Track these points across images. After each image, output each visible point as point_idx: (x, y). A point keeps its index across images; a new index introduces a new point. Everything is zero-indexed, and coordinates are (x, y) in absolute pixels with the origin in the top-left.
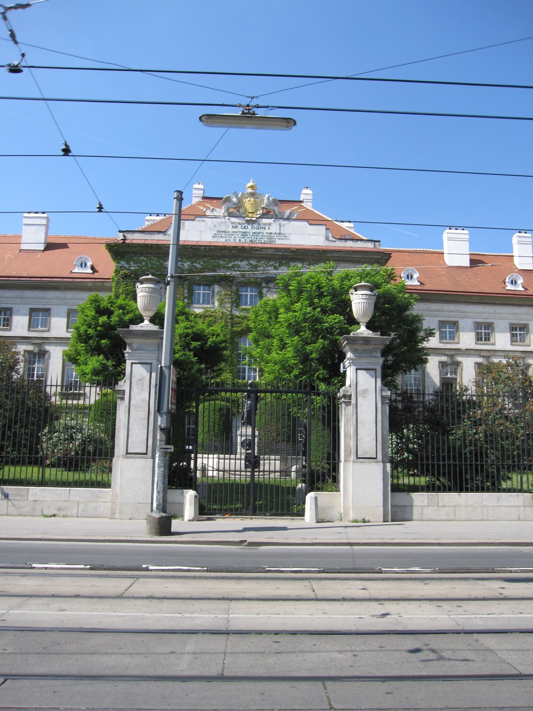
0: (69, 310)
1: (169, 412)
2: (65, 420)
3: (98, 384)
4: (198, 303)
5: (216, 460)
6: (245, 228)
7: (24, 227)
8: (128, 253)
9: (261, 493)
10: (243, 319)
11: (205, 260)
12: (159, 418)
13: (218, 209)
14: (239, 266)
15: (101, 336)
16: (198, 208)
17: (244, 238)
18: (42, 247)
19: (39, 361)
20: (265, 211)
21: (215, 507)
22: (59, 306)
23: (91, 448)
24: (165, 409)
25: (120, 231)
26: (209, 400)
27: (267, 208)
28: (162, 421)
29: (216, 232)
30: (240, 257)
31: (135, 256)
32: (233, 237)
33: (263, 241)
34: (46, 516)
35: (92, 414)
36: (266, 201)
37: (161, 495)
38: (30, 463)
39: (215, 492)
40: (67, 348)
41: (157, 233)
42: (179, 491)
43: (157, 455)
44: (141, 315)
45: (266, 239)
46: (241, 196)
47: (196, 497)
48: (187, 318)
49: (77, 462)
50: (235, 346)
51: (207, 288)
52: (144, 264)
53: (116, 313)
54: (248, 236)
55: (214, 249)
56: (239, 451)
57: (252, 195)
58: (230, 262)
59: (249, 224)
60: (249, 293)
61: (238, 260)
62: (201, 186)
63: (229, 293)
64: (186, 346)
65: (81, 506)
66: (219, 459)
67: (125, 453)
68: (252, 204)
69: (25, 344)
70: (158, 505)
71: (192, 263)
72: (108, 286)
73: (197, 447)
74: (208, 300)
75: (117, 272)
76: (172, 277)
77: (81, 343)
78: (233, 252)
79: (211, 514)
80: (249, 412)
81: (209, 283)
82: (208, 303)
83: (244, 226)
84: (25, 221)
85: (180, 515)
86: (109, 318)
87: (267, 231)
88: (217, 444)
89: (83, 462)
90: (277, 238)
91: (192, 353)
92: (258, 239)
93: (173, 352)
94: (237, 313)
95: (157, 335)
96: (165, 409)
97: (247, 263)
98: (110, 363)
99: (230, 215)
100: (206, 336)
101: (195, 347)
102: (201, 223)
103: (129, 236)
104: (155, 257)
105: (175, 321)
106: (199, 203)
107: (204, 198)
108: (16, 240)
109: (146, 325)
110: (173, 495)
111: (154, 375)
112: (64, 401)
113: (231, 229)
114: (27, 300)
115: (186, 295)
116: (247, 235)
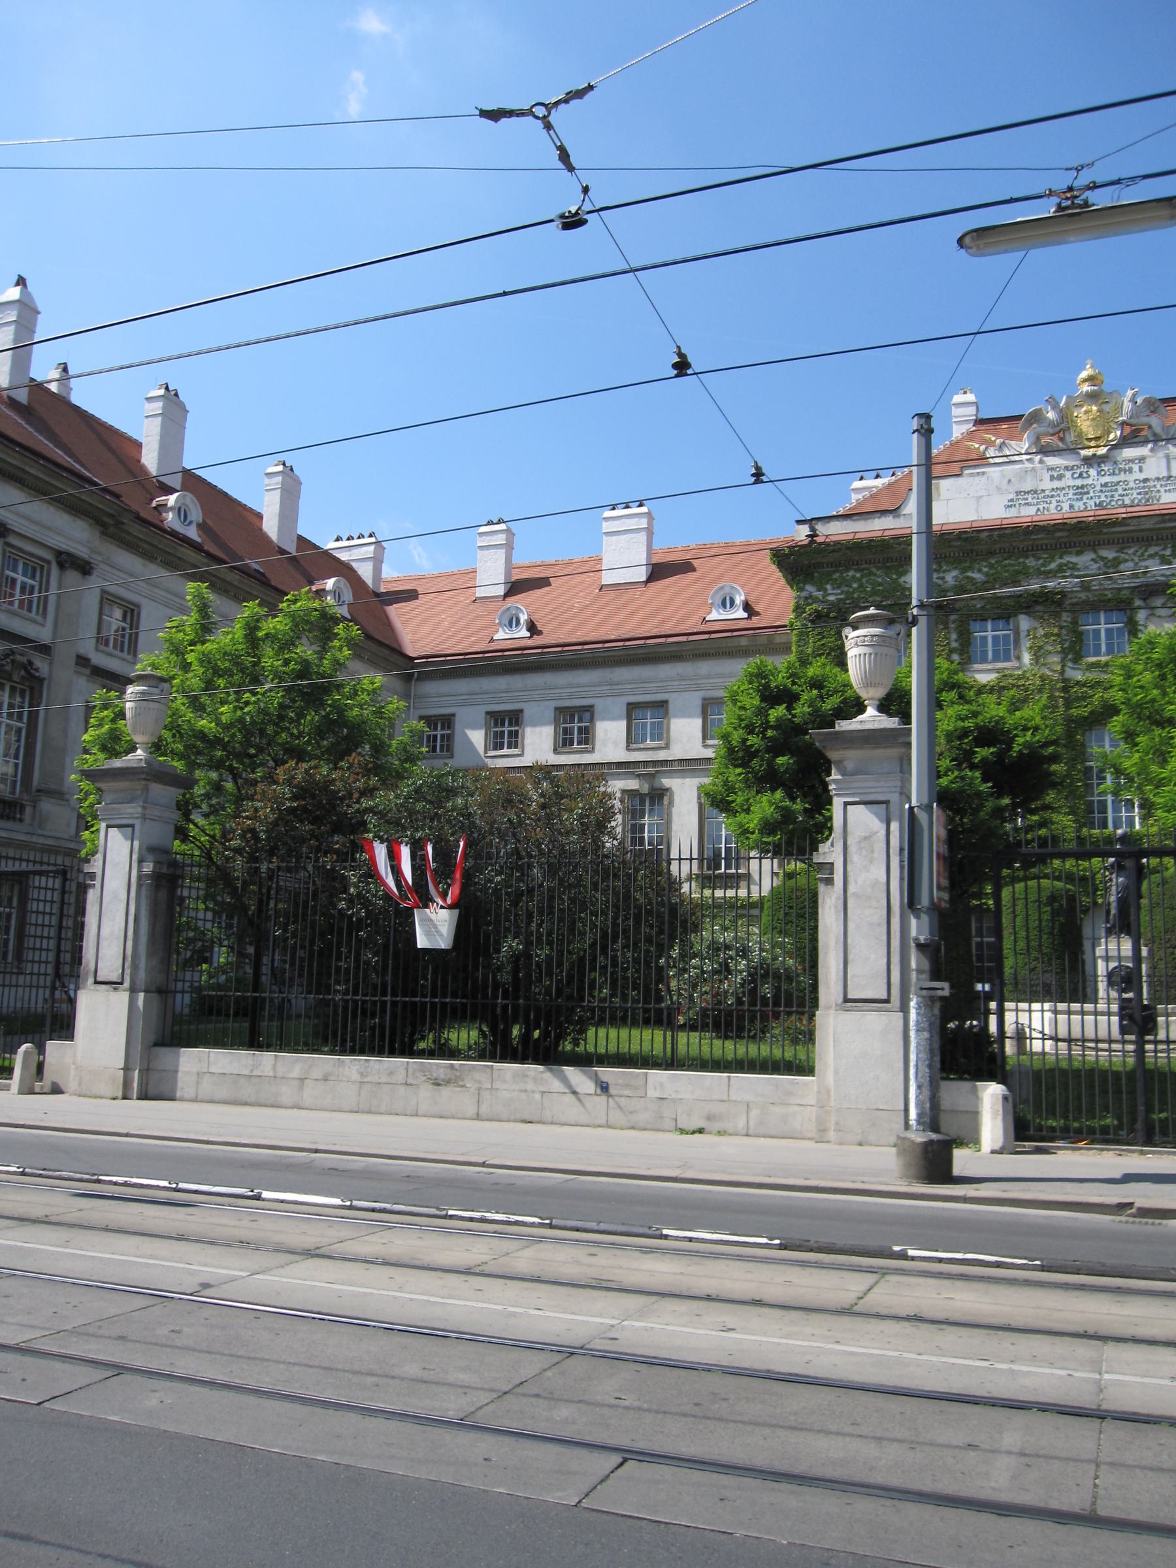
0: (704, 699)
1: (934, 907)
2: (712, 932)
3: (776, 853)
4: (984, 660)
5: (1048, 1015)
6: (1081, 476)
7: (605, 538)
8: (819, 565)
9: (1163, 1093)
10: (1092, 687)
11: (993, 561)
12: (913, 922)
13: (1013, 443)
14: (1074, 567)
15: (776, 749)
16: (967, 447)
17: (1081, 499)
18: (641, 574)
19: (651, 811)
20: (1127, 430)
21: (1052, 1123)
22: (685, 693)
23: (767, 990)
24: (925, 901)
25: (799, 522)
26: (1026, 879)
27: (1133, 421)
28: (919, 929)
29: (1011, 496)
30: (1075, 546)
31: (835, 572)
32: (1054, 500)
33: (1127, 501)
34: (683, 1131)
35: (765, 919)
36: (1127, 406)
37: (926, 1092)
38: (647, 1022)
39: (1050, 1088)
40: (707, 781)
41: (878, 515)
42: (965, 1085)
43: (913, 1004)
44: (859, 697)
45: (1135, 496)
46: (1067, 403)
47: (1005, 1098)
48: (961, 697)
49: (741, 1018)
50: (1079, 753)
51: (1001, 624)
52: (855, 585)
53: (805, 697)
54: (1092, 494)
55: (1012, 534)
56: (1102, 993)
57: (1092, 397)
58: (1052, 559)
59: (1090, 466)
60: (1102, 626)
61: (1070, 553)
62: (971, 397)
63: (1056, 630)
64: (964, 759)
65: (754, 1113)
66: (1056, 1012)
67: (841, 1000)
68: (1094, 419)
69: (623, 776)
70: (920, 1116)
73: (1002, 984)
74: (1007, 652)
75: (798, 609)
76: (921, 606)
77: (736, 766)
78: (1059, 534)
79: (1042, 1140)
80: (1123, 903)
81: (1004, 612)
82: (1007, 659)
83: (1078, 471)
84: (607, 527)
85: (971, 1139)
86: (789, 708)
88: (1051, 979)
89: (752, 1019)
90: (1162, 490)
91: (977, 774)
92: (1117, 497)
93: (935, 774)
94: (1078, 676)
95: (897, 739)
96: (925, 901)
97: (1093, 556)
98: (798, 806)
99: (1045, 451)
100: (1009, 732)
101: (984, 760)
102: (977, 479)
103: (821, 529)
104: (878, 569)
105: (936, 704)
106: (969, 436)
107: (979, 422)
108: (593, 566)
109: (871, 718)
110: (954, 1092)
111: (895, 826)
112: (707, 892)
113: (1047, 485)
114: (620, 687)
115: (954, 645)
116: (1088, 493)
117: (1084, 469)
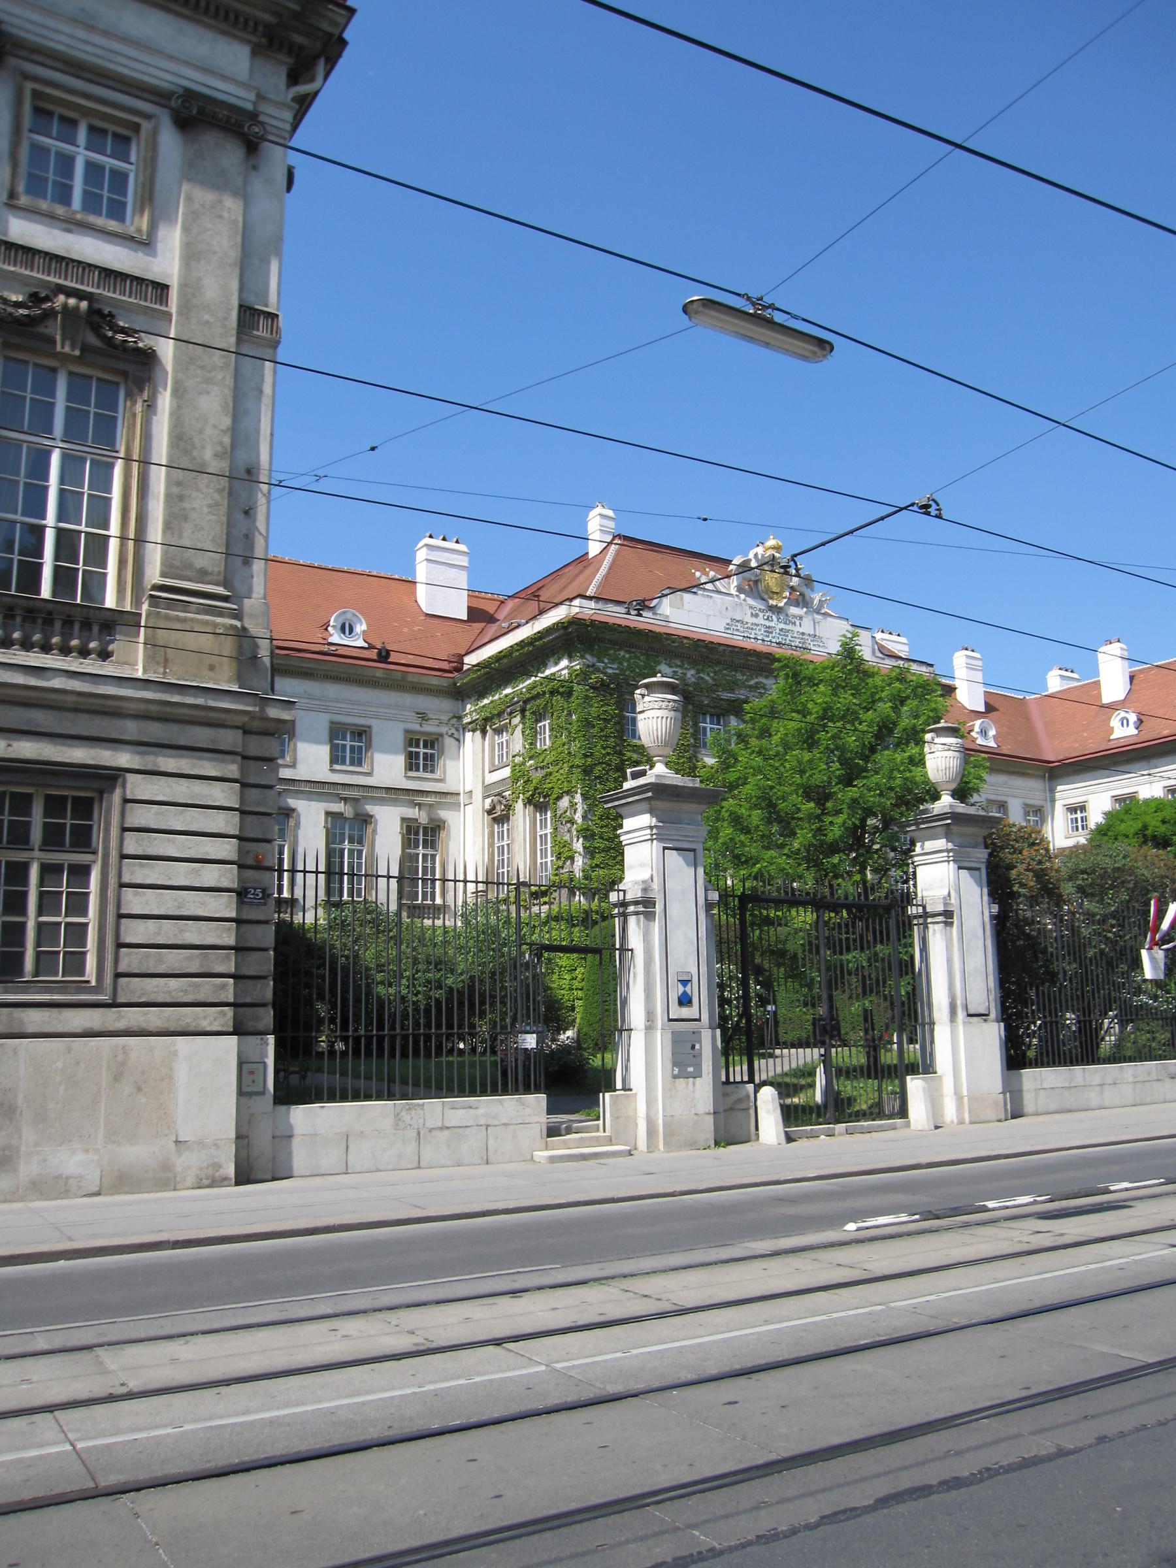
0: (332, 723)
6: (768, 619)
14: (764, 687)
29: (729, 621)
32: (753, 632)
58: (752, 678)
61: (761, 675)
71: (698, 672)
72: (415, 680)
87: (797, 629)
102: (708, 600)
104: (642, 654)
117: (769, 613)
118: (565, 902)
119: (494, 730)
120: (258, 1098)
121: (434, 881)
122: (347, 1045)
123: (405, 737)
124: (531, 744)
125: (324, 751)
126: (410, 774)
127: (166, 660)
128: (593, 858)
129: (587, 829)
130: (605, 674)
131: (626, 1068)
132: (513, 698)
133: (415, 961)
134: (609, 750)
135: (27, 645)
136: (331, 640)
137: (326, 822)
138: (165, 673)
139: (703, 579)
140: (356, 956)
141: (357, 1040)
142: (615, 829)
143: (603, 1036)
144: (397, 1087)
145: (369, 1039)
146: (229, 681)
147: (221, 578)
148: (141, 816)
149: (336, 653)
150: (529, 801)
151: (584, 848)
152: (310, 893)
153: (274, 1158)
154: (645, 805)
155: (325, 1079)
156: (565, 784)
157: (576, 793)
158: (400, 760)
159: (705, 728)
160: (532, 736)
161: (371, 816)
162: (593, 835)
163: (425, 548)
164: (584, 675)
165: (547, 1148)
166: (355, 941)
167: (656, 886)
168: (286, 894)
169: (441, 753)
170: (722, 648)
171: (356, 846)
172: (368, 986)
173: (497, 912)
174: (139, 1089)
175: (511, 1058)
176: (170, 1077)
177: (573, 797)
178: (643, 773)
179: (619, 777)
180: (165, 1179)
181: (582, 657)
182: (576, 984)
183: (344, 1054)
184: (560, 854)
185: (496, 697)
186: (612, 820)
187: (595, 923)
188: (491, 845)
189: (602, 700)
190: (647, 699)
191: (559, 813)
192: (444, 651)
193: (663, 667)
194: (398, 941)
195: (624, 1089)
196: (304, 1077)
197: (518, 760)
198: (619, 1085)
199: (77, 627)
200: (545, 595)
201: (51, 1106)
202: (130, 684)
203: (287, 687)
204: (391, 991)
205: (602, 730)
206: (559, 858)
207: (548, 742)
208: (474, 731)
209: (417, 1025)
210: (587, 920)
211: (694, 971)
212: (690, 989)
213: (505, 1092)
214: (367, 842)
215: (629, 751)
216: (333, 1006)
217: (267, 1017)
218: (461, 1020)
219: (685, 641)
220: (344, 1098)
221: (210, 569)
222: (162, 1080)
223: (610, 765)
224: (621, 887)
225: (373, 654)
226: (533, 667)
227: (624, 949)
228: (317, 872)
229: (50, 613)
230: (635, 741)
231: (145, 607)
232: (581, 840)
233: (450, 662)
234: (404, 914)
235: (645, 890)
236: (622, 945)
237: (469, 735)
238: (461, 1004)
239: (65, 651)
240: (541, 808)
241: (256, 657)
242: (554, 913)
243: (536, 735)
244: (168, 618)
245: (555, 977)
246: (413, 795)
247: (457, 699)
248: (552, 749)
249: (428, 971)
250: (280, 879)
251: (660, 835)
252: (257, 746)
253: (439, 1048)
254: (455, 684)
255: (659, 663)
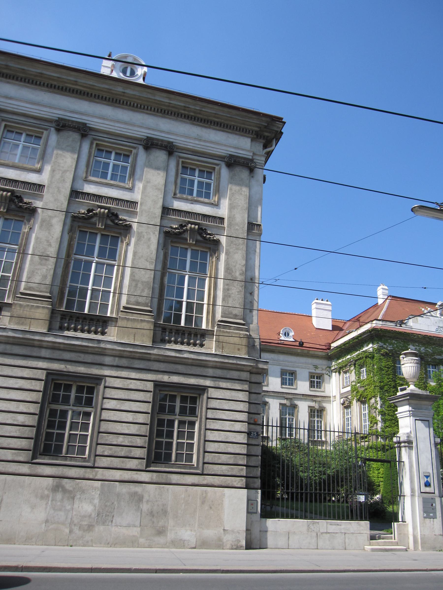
0: (282, 369)
11: (433, 347)
29: (437, 327)
31: (390, 339)
71: (426, 348)
102: (428, 319)
104: (402, 341)
118: (375, 441)
119: (344, 372)
120: (255, 515)
121: (321, 431)
122: (288, 495)
123: (309, 375)
124: (358, 377)
125: (279, 380)
126: (311, 389)
127: (223, 347)
128: (385, 423)
129: (382, 412)
130: (387, 349)
131: (403, 513)
132: (351, 359)
133: (315, 463)
134: (390, 380)
135: (176, 342)
136: (281, 339)
137: (280, 407)
138: (222, 351)
139: (426, 312)
140: (292, 460)
141: (292, 494)
142: (394, 411)
143: (392, 497)
144: (308, 514)
145: (297, 493)
146: (245, 354)
147: (242, 317)
148: (213, 404)
149: (283, 343)
150: (358, 400)
151: (382, 419)
152: (274, 435)
153: (260, 540)
154: (406, 402)
155: (280, 509)
156: (373, 393)
157: (377, 397)
158: (307, 384)
159: (430, 371)
160: (358, 374)
161: (297, 405)
162: (385, 414)
163: (315, 304)
164: (378, 350)
165: (370, 545)
166: (291, 454)
167: (413, 435)
168: (265, 435)
169: (323, 381)
170: (435, 338)
171: (291, 417)
172: (296, 472)
173: (347, 444)
174: (211, 508)
175: (354, 505)
176: (222, 504)
177: (376, 398)
178: (405, 389)
179: (395, 390)
180: (219, 545)
181: (378, 343)
182: (380, 475)
183: (287, 499)
184: (371, 421)
185: (344, 359)
186: (393, 408)
187: (387, 450)
188: (344, 417)
189: (386, 360)
190: (405, 359)
191: (371, 405)
192: (323, 342)
193: (411, 346)
194: (308, 454)
195: (403, 521)
196: (271, 508)
197: (353, 384)
198: (400, 519)
199: (193, 335)
200: (361, 320)
201: (179, 512)
202: (210, 356)
203: (265, 356)
204: (306, 474)
205: (387, 372)
206: (371, 423)
207: (365, 377)
208: (336, 372)
209: (316, 489)
210: (383, 448)
211: (431, 471)
212: (431, 480)
213: (352, 519)
214: (295, 415)
215: (398, 380)
216: (283, 479)
217: (258, 483)
218: (334, 488)
219: (419, 336)
220: (287, 517)
221: (238, 314)
222: (219, 505)
223: (391, 386)
224: (398, 435)
225: (297, 344)
226: (358, 347)
227: (400, 461)
228: (277, 426)
229: (184, 331)
230: (402, 376)
231: (216, 328)
232: (380, 416)
233: (326, 346)
234: (310, 444)
235: (408, 437)
236: (399, 459)
237: (334, 374)
238: (333, 482)
239: (189, 344)
240: (363, 403)
241: (254, 345)
242: (370, 445)
243: (360, 374)
244: (223, 332)
245: (371, 472)
246: (313, 397)
247: (329, 360)
248: (367, 379)
249: (320, 467)
250: (263, 429)
251: (413, 414)
252: (255, 378)
253: (325, 499)
254: (328, 354)
255: (409, 345)
